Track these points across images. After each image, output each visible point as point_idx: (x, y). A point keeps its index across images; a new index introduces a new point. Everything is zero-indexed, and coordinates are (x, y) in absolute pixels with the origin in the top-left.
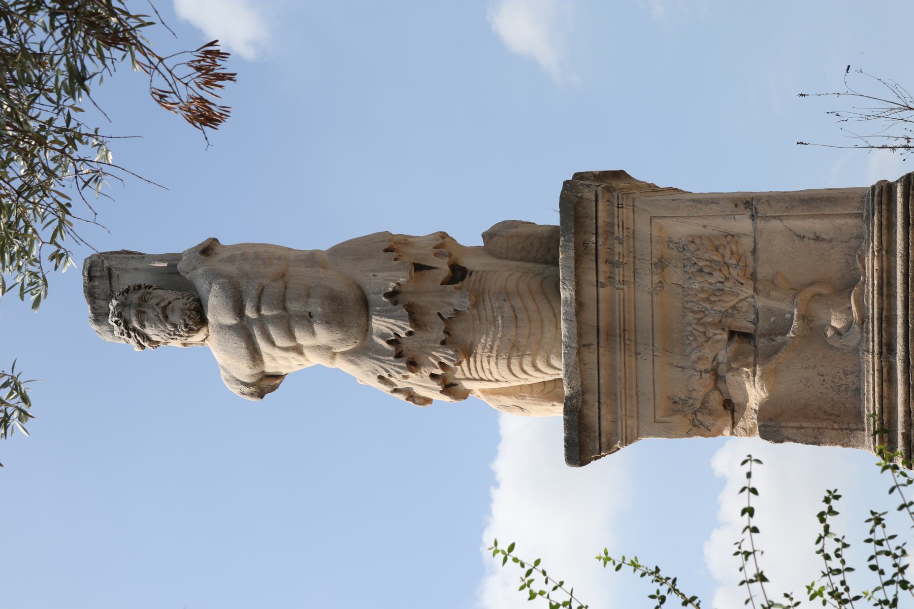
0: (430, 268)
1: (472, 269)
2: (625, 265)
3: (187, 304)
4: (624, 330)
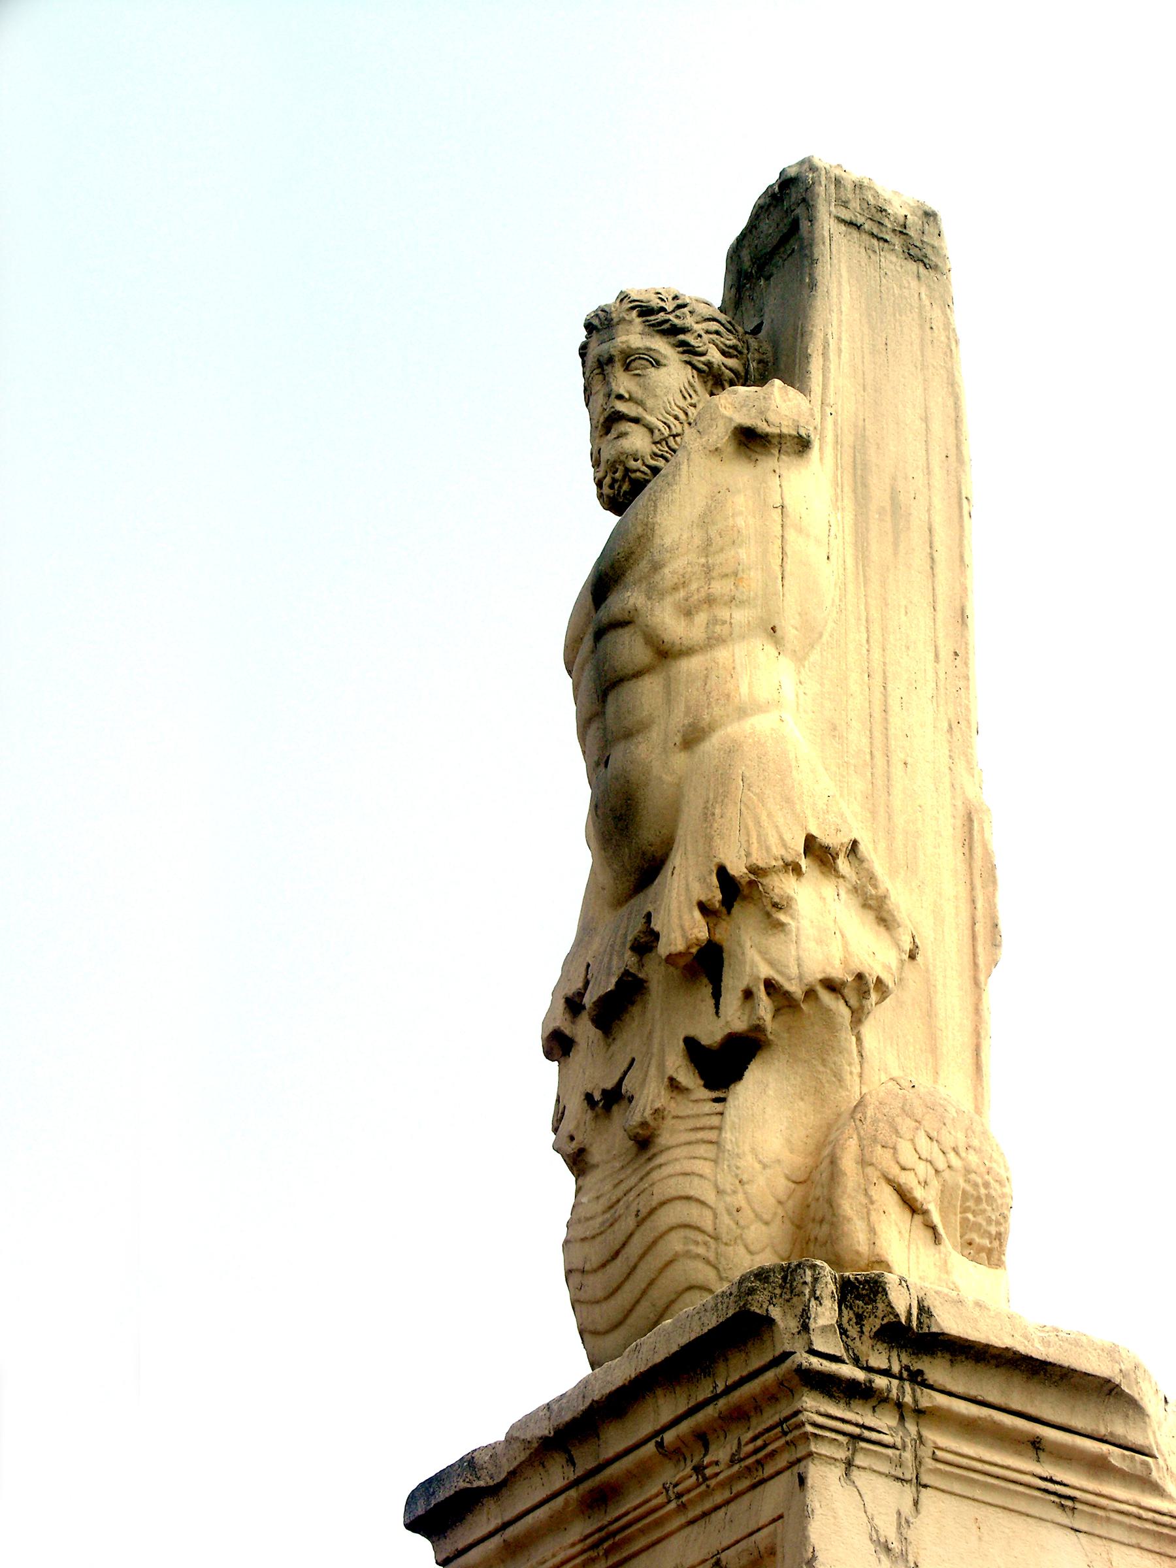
0: (717, 995)
1: (730, 1099)
2: (703, 1487)
3: (636, 460)
4: (613, 1534)
